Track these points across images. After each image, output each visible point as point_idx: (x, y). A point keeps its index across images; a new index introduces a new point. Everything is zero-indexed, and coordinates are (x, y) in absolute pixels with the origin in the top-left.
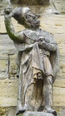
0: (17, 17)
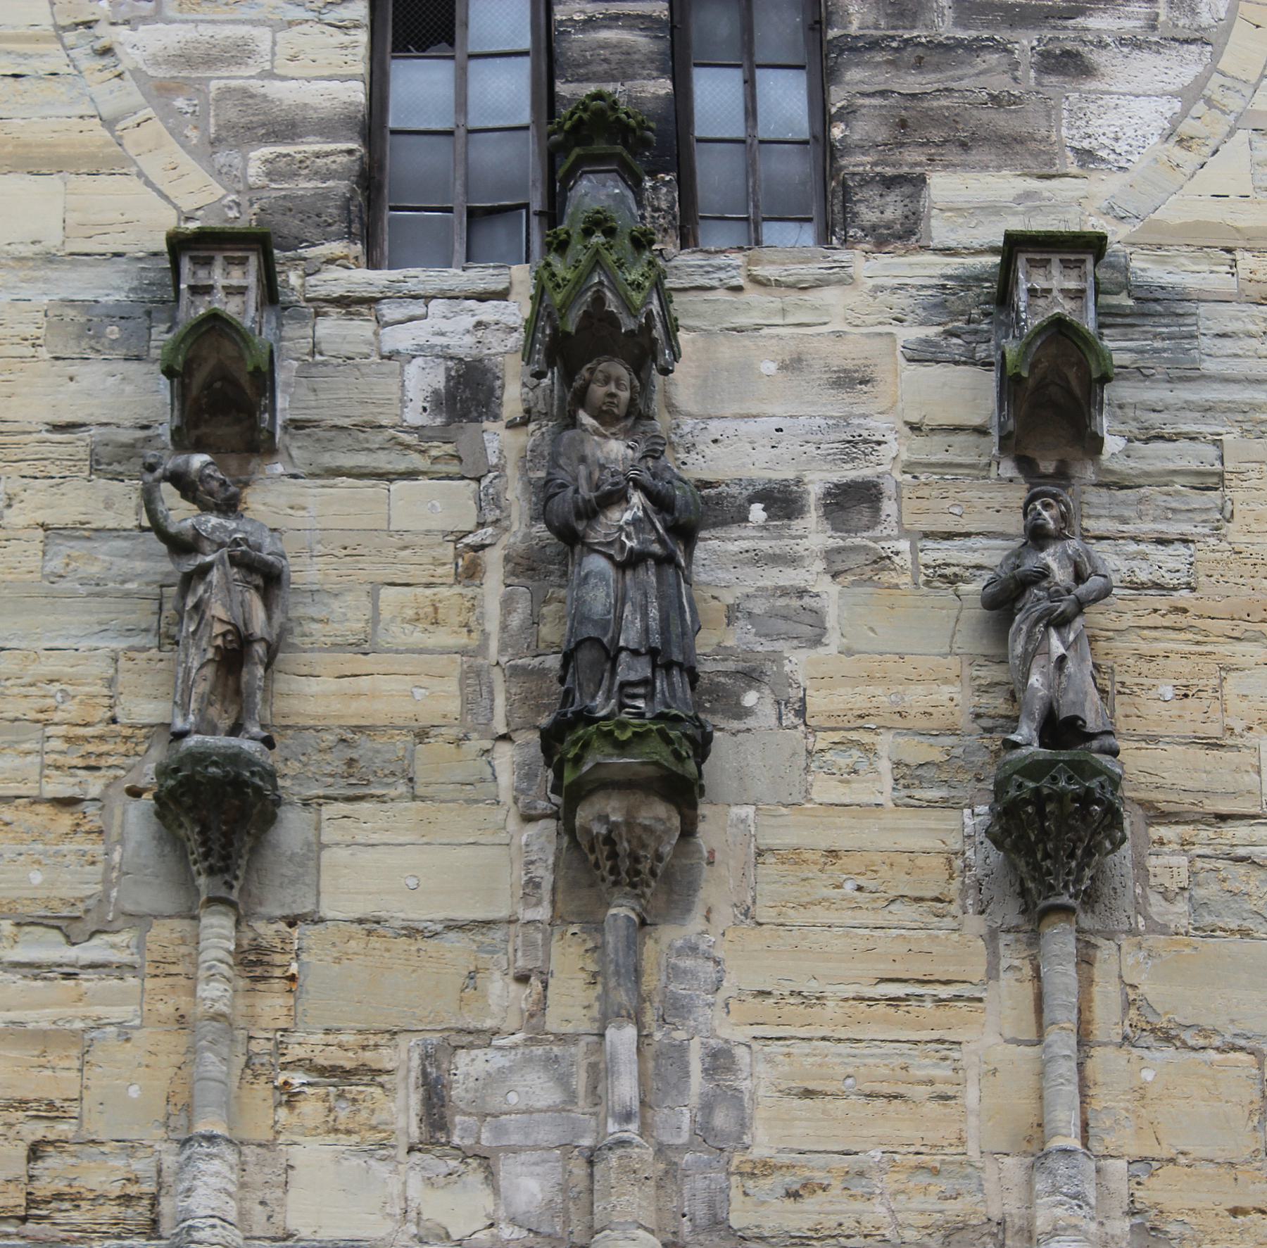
0: (179, 480)
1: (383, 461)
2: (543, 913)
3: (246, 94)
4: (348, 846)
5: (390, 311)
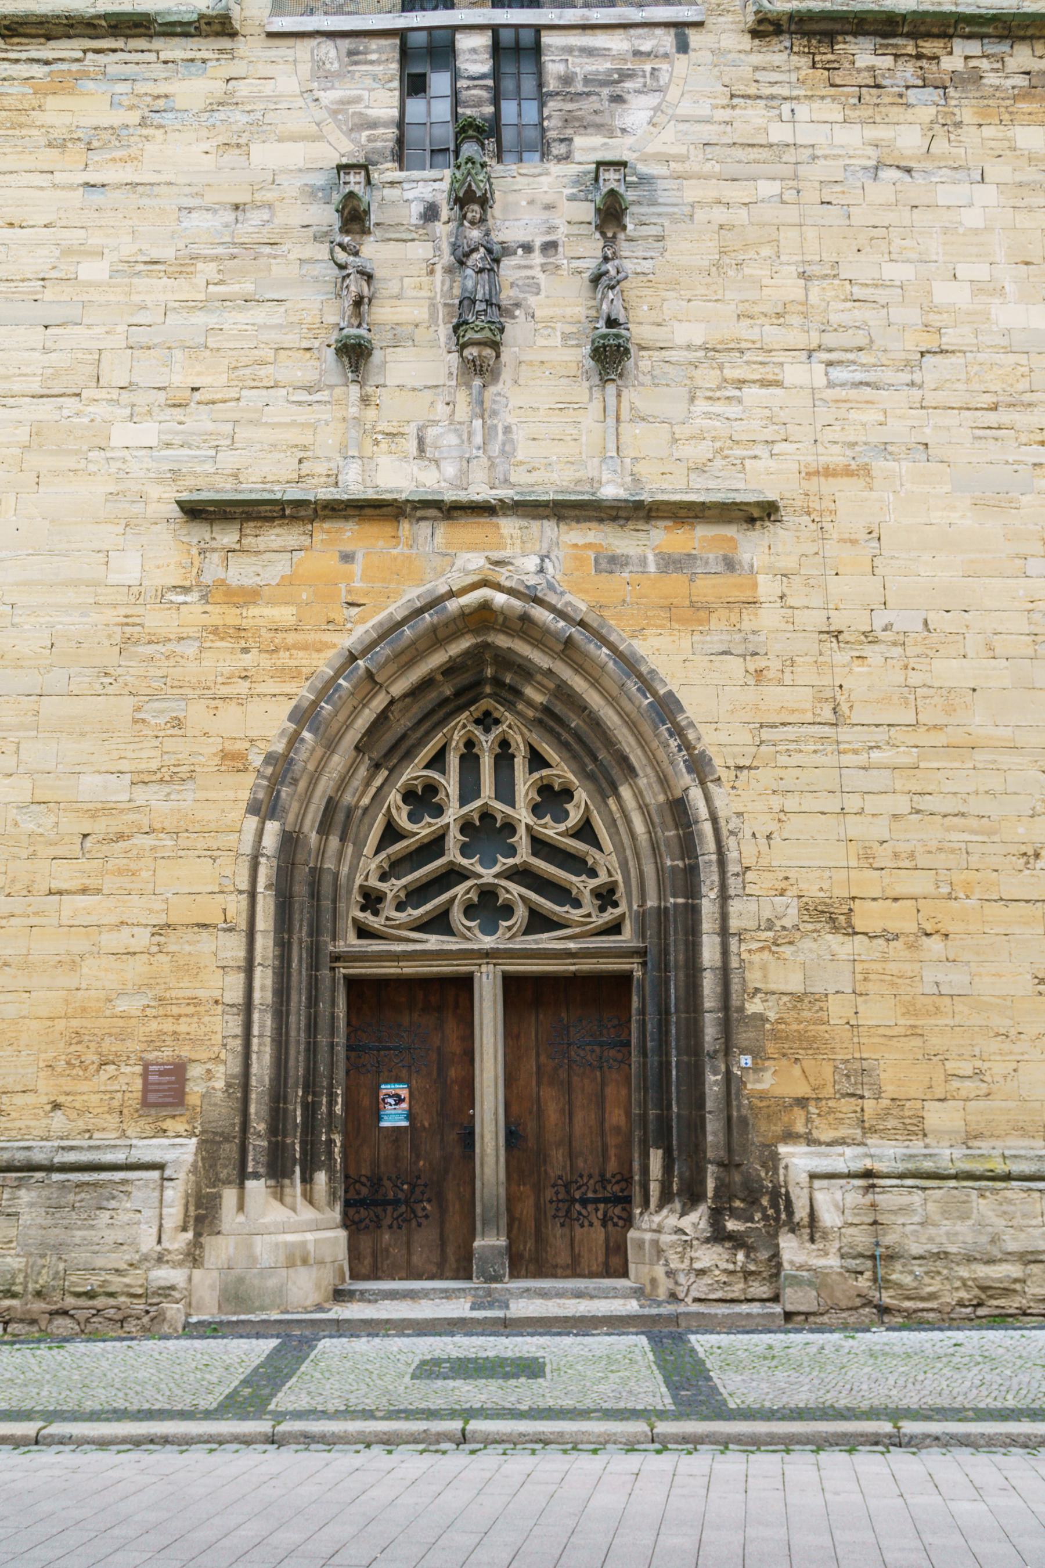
1: (404, 236)
2: (454, 383)
3: (361, 114)
5: (406, 186)
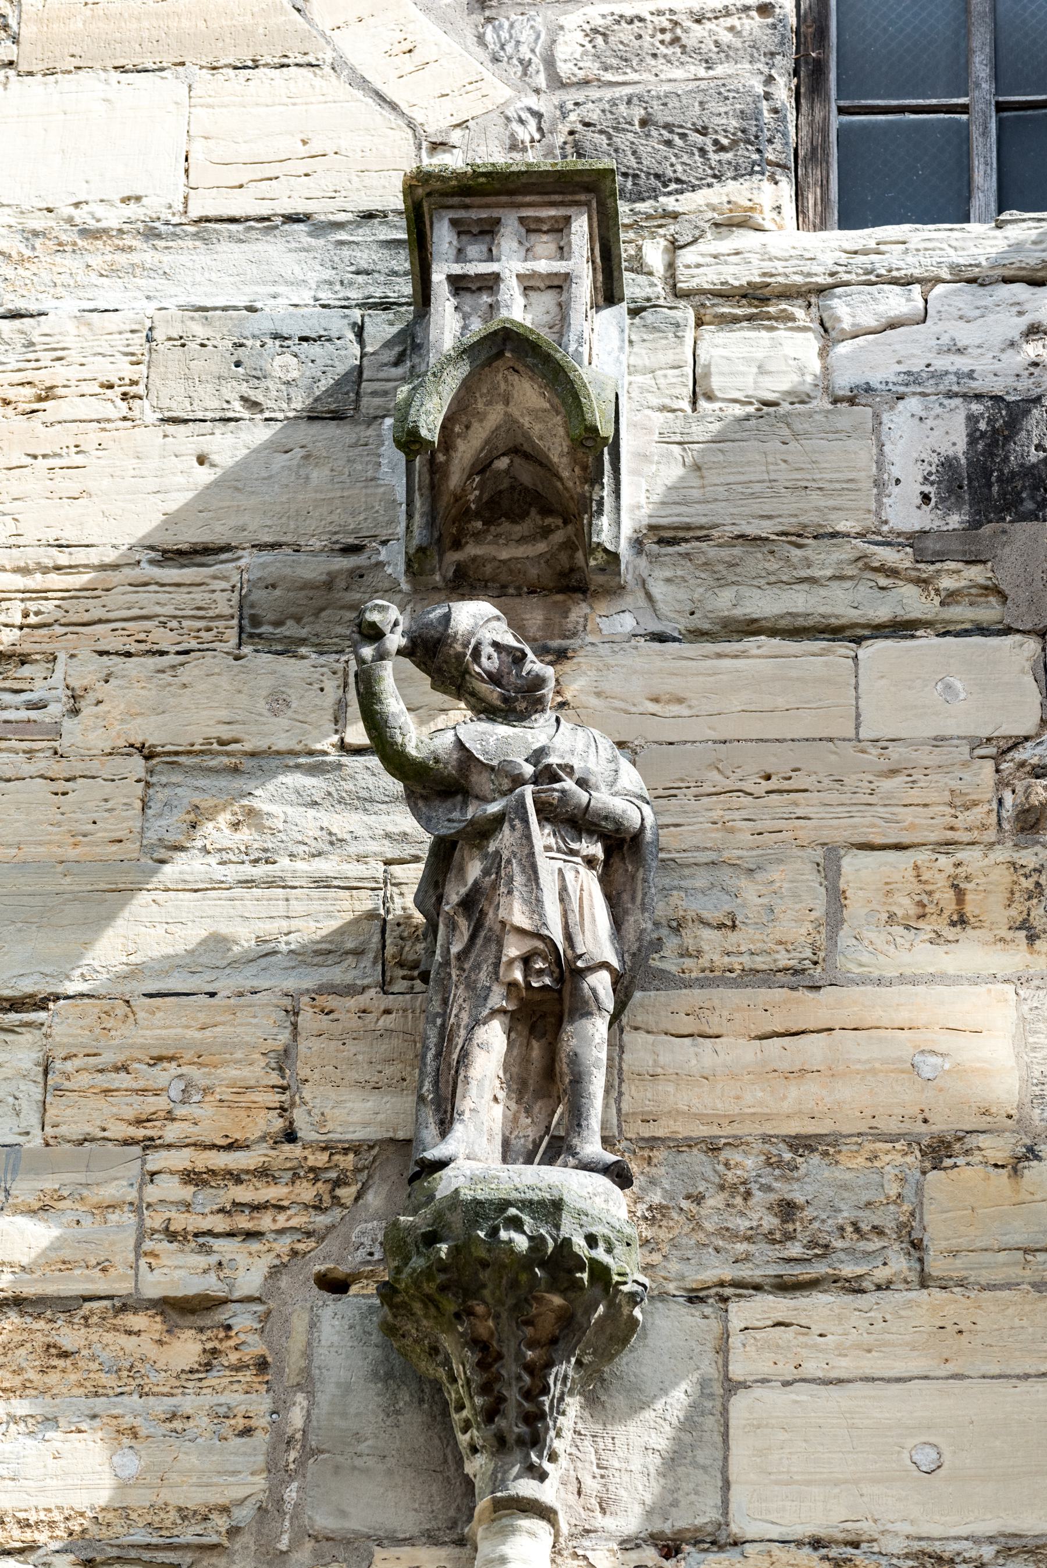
4: (786, 1384)
